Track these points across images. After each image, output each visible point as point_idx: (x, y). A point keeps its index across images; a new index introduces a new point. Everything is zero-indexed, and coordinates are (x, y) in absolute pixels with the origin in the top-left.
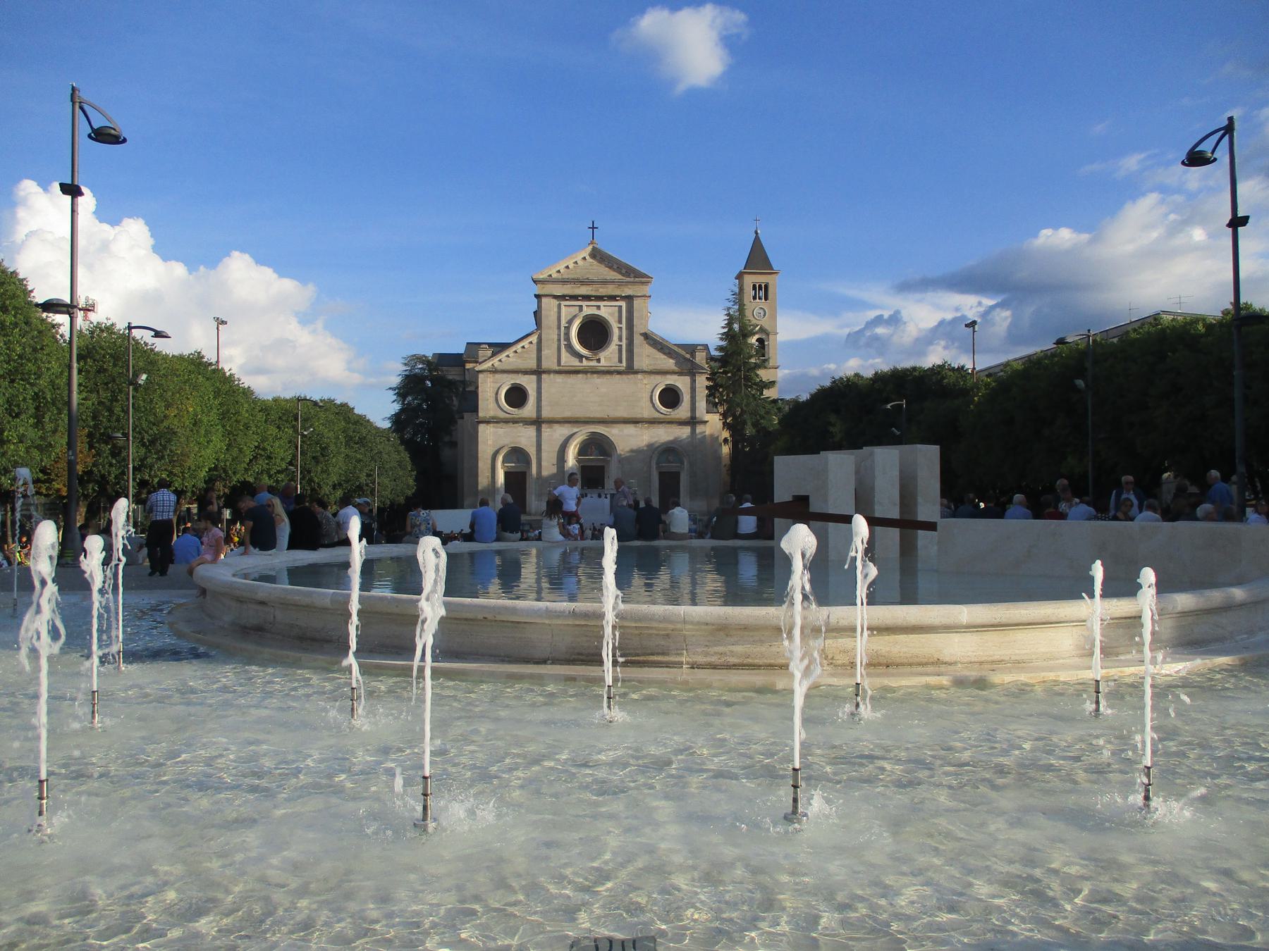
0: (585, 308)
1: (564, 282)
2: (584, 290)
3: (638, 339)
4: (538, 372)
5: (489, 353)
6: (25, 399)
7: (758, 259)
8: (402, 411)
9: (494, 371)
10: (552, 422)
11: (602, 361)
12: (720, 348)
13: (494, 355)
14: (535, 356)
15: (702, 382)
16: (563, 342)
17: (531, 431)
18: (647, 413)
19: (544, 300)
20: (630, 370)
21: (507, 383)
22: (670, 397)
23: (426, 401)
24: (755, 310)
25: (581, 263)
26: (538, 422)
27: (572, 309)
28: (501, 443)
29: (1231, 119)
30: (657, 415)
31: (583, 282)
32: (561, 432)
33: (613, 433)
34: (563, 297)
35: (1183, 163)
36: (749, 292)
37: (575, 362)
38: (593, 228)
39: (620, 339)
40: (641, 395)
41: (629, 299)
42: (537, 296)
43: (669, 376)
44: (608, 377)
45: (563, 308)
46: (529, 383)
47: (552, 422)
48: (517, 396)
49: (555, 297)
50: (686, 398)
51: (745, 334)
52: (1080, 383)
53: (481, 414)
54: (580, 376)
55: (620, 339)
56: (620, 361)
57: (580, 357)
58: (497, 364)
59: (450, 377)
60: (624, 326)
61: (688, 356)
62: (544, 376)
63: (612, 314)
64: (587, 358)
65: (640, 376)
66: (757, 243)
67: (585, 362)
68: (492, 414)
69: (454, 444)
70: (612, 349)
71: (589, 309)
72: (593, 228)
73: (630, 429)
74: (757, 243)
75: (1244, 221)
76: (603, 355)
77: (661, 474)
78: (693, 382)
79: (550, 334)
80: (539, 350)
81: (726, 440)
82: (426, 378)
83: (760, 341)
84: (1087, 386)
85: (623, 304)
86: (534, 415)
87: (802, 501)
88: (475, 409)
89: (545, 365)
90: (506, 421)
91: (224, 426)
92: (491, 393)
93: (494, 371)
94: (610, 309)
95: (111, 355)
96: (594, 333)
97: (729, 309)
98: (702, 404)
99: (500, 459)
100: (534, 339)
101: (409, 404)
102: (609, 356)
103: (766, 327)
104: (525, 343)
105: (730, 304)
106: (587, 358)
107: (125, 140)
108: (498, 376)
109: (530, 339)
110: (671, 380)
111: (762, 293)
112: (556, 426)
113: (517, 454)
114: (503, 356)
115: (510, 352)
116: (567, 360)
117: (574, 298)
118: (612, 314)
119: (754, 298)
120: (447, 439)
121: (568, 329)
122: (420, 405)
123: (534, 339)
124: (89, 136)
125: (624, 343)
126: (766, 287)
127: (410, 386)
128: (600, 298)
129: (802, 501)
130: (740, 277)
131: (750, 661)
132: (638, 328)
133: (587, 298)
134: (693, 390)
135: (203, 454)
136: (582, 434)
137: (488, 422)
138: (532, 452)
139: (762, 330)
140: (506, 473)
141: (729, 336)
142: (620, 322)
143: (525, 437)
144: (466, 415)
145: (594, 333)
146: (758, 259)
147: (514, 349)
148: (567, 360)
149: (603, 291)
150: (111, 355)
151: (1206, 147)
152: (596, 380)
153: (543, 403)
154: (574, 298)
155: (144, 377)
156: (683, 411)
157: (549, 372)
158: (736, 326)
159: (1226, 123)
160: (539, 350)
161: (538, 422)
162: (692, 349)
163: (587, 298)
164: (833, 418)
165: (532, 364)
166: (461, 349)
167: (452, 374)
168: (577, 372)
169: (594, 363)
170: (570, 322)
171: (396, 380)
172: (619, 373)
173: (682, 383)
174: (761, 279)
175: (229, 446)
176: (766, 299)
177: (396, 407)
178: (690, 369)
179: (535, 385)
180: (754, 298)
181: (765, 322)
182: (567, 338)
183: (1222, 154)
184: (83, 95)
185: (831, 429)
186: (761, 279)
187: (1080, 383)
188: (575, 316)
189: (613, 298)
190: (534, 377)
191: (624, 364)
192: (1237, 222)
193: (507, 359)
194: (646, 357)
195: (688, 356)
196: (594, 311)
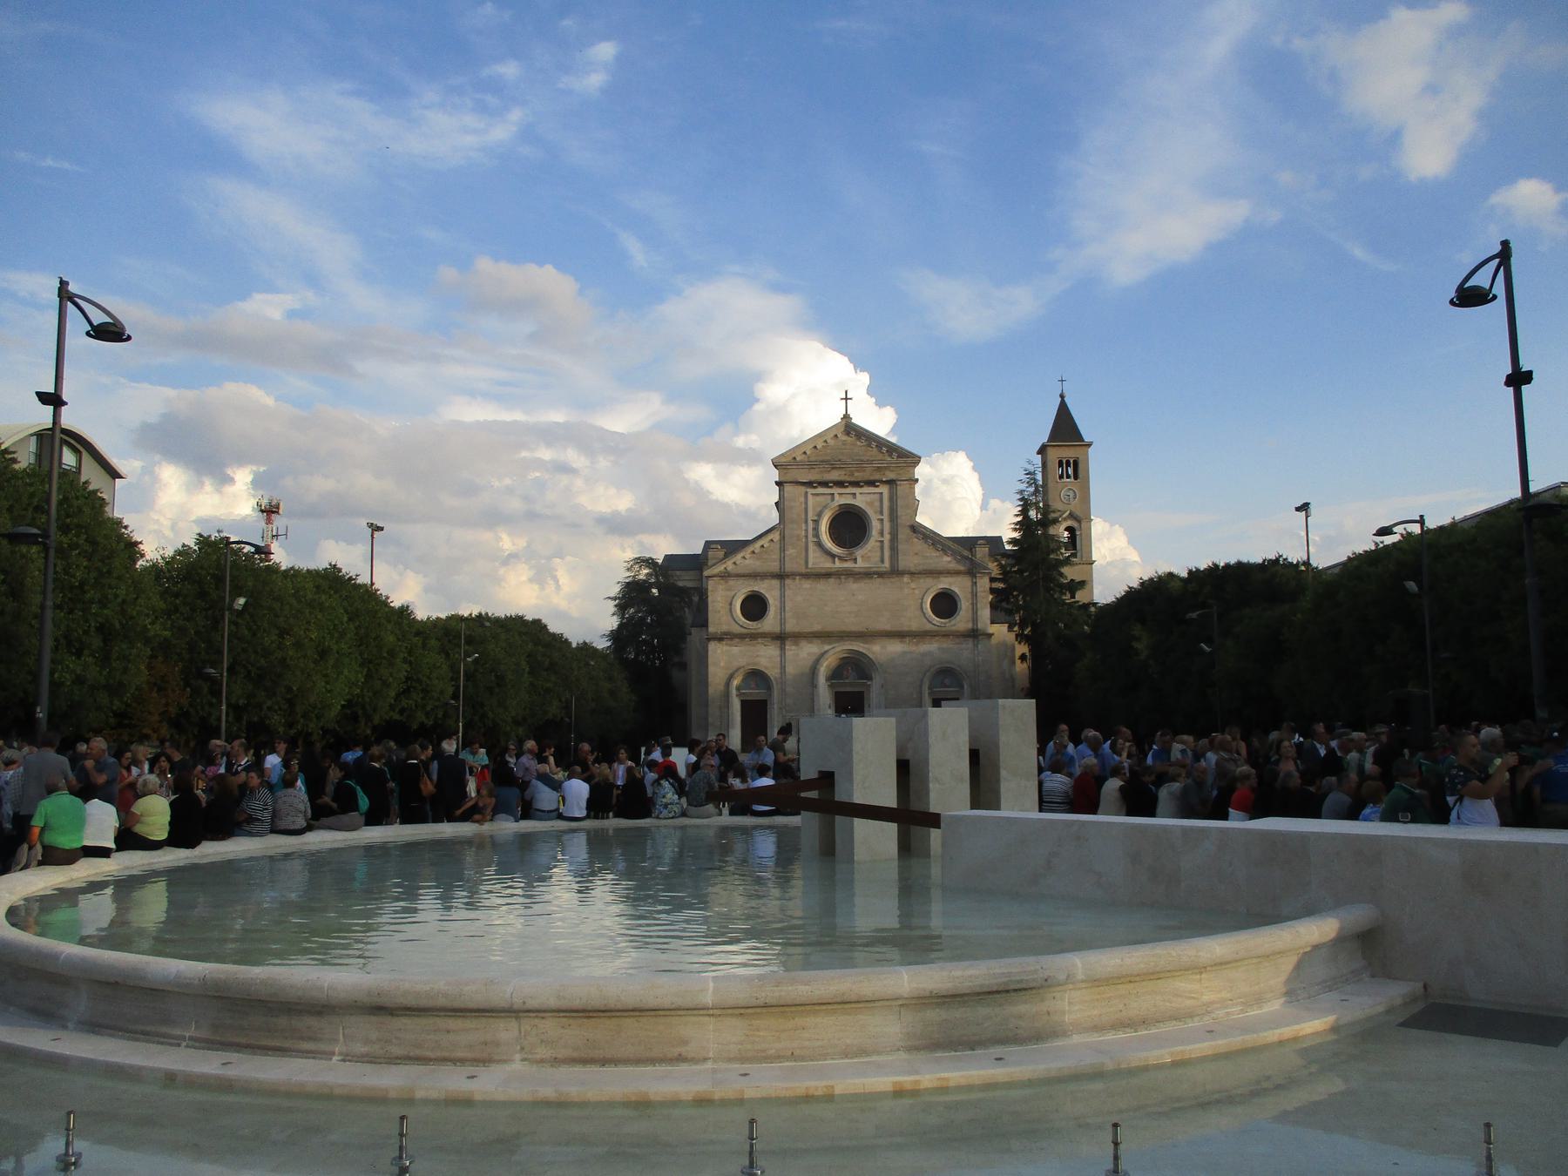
1: (811, 465)
2: (835, 475)
3: (904, 533)
4: (781, 576)
5: (721, 554)
6: (86, 632)
7: (1065, 428)
8: (621, 626)
9: (725, 576)
10: (798, 637)
11: (859, 560)
12: (1013, 541)
13: (726, 556)
14: (776, 556)
15: (984, 583)
16: (811, 538)
18: (915, 624)
19: (788, 488)
20: (895, 572)
21: (742, 591)
22: (945, 604)
23: (650, 613)
24: (1062, 495)
26: (781, 638)
27: (818, 499)
28: (736, 664)
29: (1505, 244)
30: (929, 627)
32: (808, 650)
34: (810, 484)
35: (1452, 303)
37: (827, 564)
39: (882, 534)
40: (910, 604)
41: (891, 482)
45: (811, 499)
46: (769, 590)
47: (798, 637)
48: (755, 607)
49: (803, 484)
50: (964, 605)
51: (1046, 522)
52: (1412, 586)
53: (711, 629)
54: (832, 580)
55: (882, 534)
56: (882, 561)
57: (833, 556)
59: (681, 584)
60: (886, 517)
61: (966, 553)
62: (788, 582)
65: (906, 579)
67: (838, 564)
68: (725, 628)
69: (683, 666)
70: (872, 544)
71: (842, 498)
73: (895, 647)
75: (1527, 377)
76: (859, 553)
80: (783, 549)
81: (1023, 657)
82: (652, 585)
83: (1070, 529)
84: (1420, 587)
85: (884, 490)
86: (777, 630)
87: (826, 779)
88: (704, 624)
89: (789, 567)
90: (742, 637)
91: (361, 654)
92: (724, 604)
93: (725, 576)
94: (868, 498)
95: (213, 576)
96: (849, 527)
97: (1021, 492)
98: (985, 613)
99: (736, 682)
100: (776, 536)
101: (631, 618)
102: (868, 554)
103: (1078, 513)
104: (765, 541)
105: (1023, 486)
106: (841, 558)
107: (129, 338)
108: (732, 582)
109: (770, 536)
111: (1070, 471)
113: (756, 676)
114: (738, 558)
115: (747, 552)
116: (817, 561)
118: (871, 504)
119: (1061, 477)
120: (676, 659)
121: (816, 522)
122: (643, 619)
123: (776, 536)
124: (88, 333)
125: (887, 537)
127: (632, 595)
128: (856, 484)
129: (826, 779)
130: (1042, 451)
131: (418, 1052)
132: (903, 520)
134: (974, 595)
135: (334, 689)
136: (833, 654)
138: (773, 673)
139: (1072, 516)
140: (744, 704)
141: (1025, 525)
142: (881, 513)
143: (765, 657)
144: (693, 630)
146: (1065, 428)
147: (750, 549)
149: (858, 476)
150: (213, 576)
151: (1482, 280)
152: (854, 586)
153: (788, 615)
154: (824, 484)
155: (242, 601)
156: (961, 622)
157: (792, 575)
158: (1032, 514)
159: (1499, 248)
160: (783, 549)
161: (781, 638)
162: (969, 543)
163: (840, 484)
164: (1137, 630)
165: (774, 566)
166: (697, 549)
167: (684, 580)
168: (827, 575)
170: (820, 515)
171: (615, 590)
172: (881, 575)
173: (958, 586)
174: (1068, 453)
175: (368, 676)
177: (613, 623)
178: (973, 571)
179: (777, 593)
180: (1061, 477)
181: (1075, 506)
182: (817, 535)
183: (1499, 289)
184: (72, 288)
185: (1136, 645)
186: (1068, 453)
187: (1412, 586)
188: (825, 507)
189: (872, 483)
190: (776, 583)
191: (887, 564)
192: (1518, 378)
193: (743, 561)
195: (966, 553)
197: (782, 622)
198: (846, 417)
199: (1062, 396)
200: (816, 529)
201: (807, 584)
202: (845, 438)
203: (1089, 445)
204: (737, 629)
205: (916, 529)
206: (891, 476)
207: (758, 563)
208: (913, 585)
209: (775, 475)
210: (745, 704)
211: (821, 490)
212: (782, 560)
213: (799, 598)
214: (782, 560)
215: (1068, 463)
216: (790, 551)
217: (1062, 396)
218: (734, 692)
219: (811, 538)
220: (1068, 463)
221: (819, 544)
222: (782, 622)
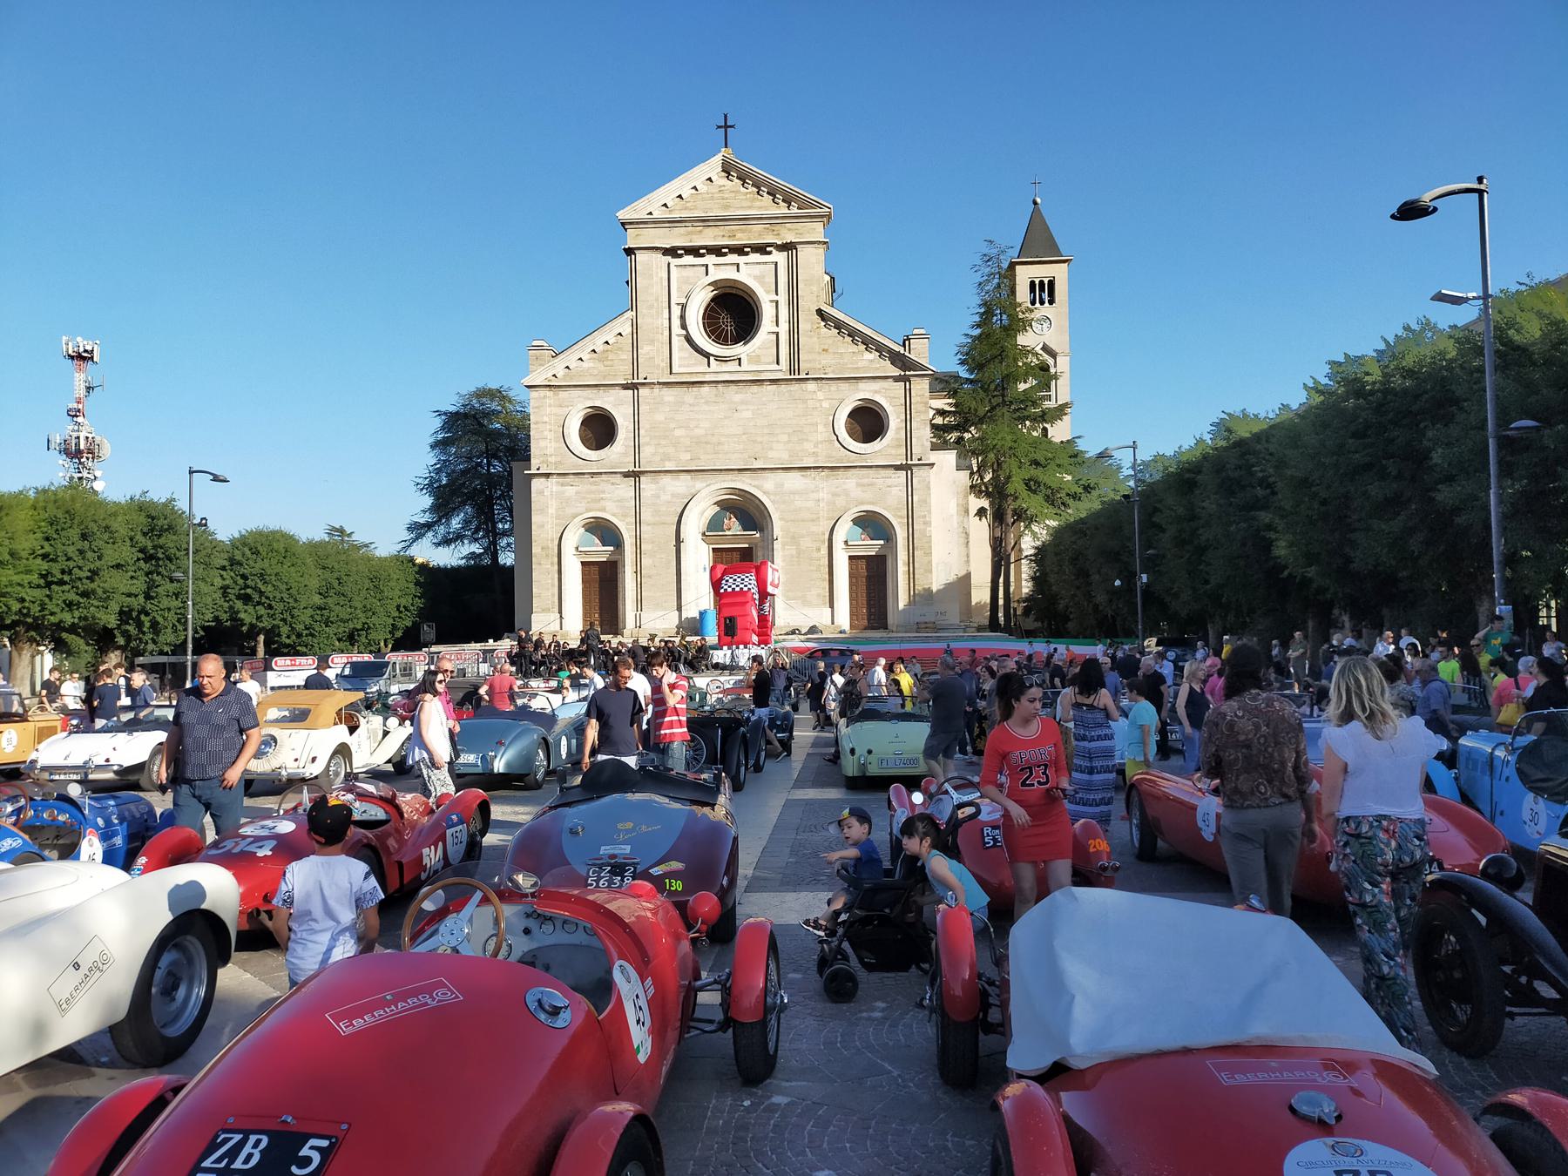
0: (711, 268)
3: (808, 321)
17: (626, 488)
19: (641, 257)
20: (796, 375)
22: (868, 422)
25: (702, 188)
27: (689, 272)
31: (705, 221)
33: (763, 489)
34: (672, 252)
36: (1023, 294)
38: (726, 127)
41: (787, 247)
42: (630, 252)
43: (862, 385)
44: (755, 388)
46: (618, 406)
48: (599, 429)
57: (707, 355)
58: (561, 373)
60: (783, 298)
62: (643, 391)
63: (758, 278)
64: (718, 358)
65: (811, 386)
66: (1036, 215)
72: (726, 127)
73: (794, 481)
74: (1036, 215)
78: (908, 393)
79: (654, 318)
80: (635, 346)
85: (780, 257)
94: (757, 270)
96: (733, 314)
98: (923, 435)
102: (756, 353)
106: (718, 358)
108: (563, 394)
110: (867, 391)
111: (1046, 296)
112: (666, 479)
117: (694, 251)
121: (684, 307)
125: (784, 328)
126: (1052, 283)
128: (739, 250)
133: (717, 251)
137: (547, 475)
143: (614, 503)
148: (686, 363)
152: (735, 395)
154: (694, 251)
160: (635, 346)
161: (635, 475)
163: (717, 251)
169: (733, 366)
170: (688, 297)
173: (888, 397)
176: (1051, 302)
182: (684, 326)
189: (761, 249)
194: (824, 350)
196: (729, 274)
197: (637, 448)
200: (683, 317)
201: (670, 395)
204: (571, 465)
206: (789, 238)
207: (600, 366)
208: (820, 395)
211: (689, 259)
212: (635, 362)
213: (660, 417)
214: (635, 362)
215: (1042, 283)
216: (644, 350)
217: (1035, 203)
220: (1042, 283)
221: (689, 339)
222: (637, 448)
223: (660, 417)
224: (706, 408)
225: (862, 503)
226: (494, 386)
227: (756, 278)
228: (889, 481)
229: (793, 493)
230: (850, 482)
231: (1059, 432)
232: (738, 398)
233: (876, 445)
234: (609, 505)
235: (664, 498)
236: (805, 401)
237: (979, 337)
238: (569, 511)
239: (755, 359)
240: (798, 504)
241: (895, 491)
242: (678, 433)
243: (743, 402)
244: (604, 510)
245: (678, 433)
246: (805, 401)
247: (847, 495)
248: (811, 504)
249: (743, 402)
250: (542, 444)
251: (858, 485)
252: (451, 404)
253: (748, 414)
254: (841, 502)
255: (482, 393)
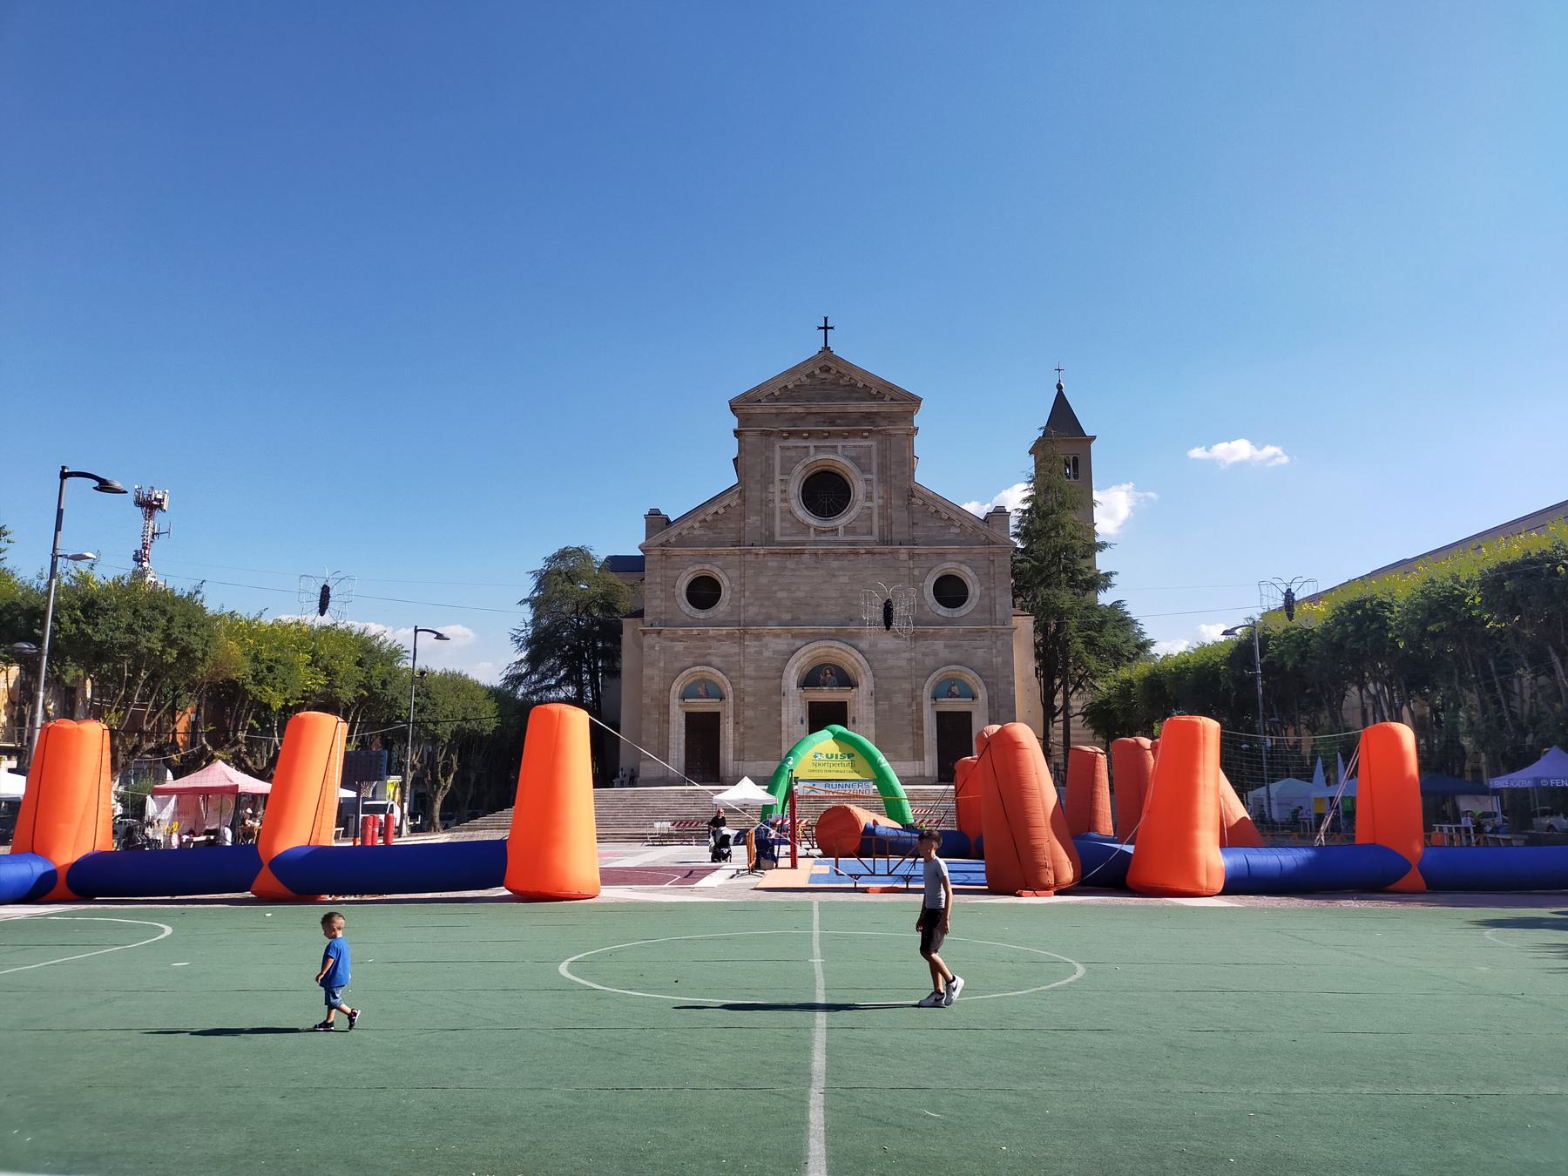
0: (812, 450)
19: (751, 439)
22: (950, 591)
27: (788, 453)
38: (826, 328)
39: (869, 497)
44: (852, 557)
48: (704, 592)
50: (974, 589)
57: (808, 526)
60: (874, 477)
72: (826, 328)
76: (841, 522)
77: (941, 717)
96: (827, 492)
125: (876, 503)
126: (1075, 460)
145: (827, 492)
160: (743, 517)
179: (735, 573)
191: (875, 537)
198: (826, 348)
199: (1059, 387)
202: (824, 376)
203: (1094, 438)
205: (912, 493)
209: (734, 422)
210: (691, 718)
211: (792, 442)
213: (763, 580)
216: (753, 520)
217: (1059, 387)
218: (675, 702)
219: (778, 504)
223: (763, 580)
224: (805, 572)
225: (950, 663)
226: (575, 545)
227: (852, 459)
228: (974, 644)
229: (887, 652)
230: (939, 645)
231: (1105, 598)
232: (835, 564)
233: (963, 611)
234: (715, 660)
235: (767, 654)
236: (897, 569)
237: (1029, 511)
238: (677, 665)
239: (849, 530)
240: (891, 662)
241: (980, 652)
242: (781, 595)
243: (840, 569)
244: (709, 665)
245: (781, 595)
246: (897, 569)
247: (936, 654)
248: (903, 663)
249: (840, 569)
250: (656, 603)
251: (946, 646)
252: (540, 565)
253: (846, 579)
254: (930, 661)
255: (563, 555)
